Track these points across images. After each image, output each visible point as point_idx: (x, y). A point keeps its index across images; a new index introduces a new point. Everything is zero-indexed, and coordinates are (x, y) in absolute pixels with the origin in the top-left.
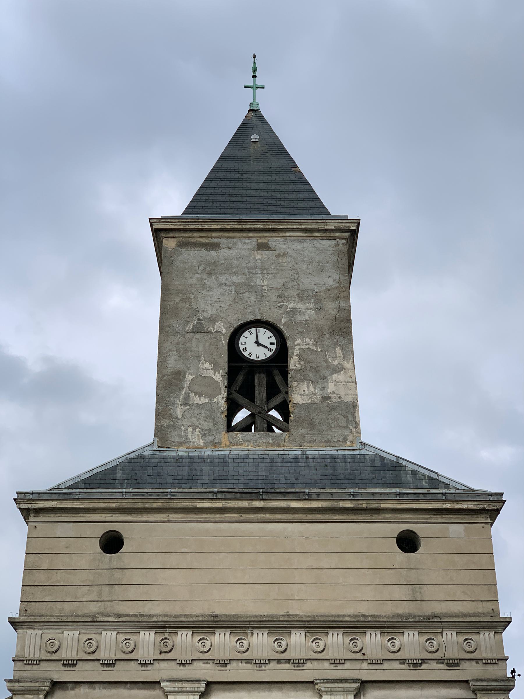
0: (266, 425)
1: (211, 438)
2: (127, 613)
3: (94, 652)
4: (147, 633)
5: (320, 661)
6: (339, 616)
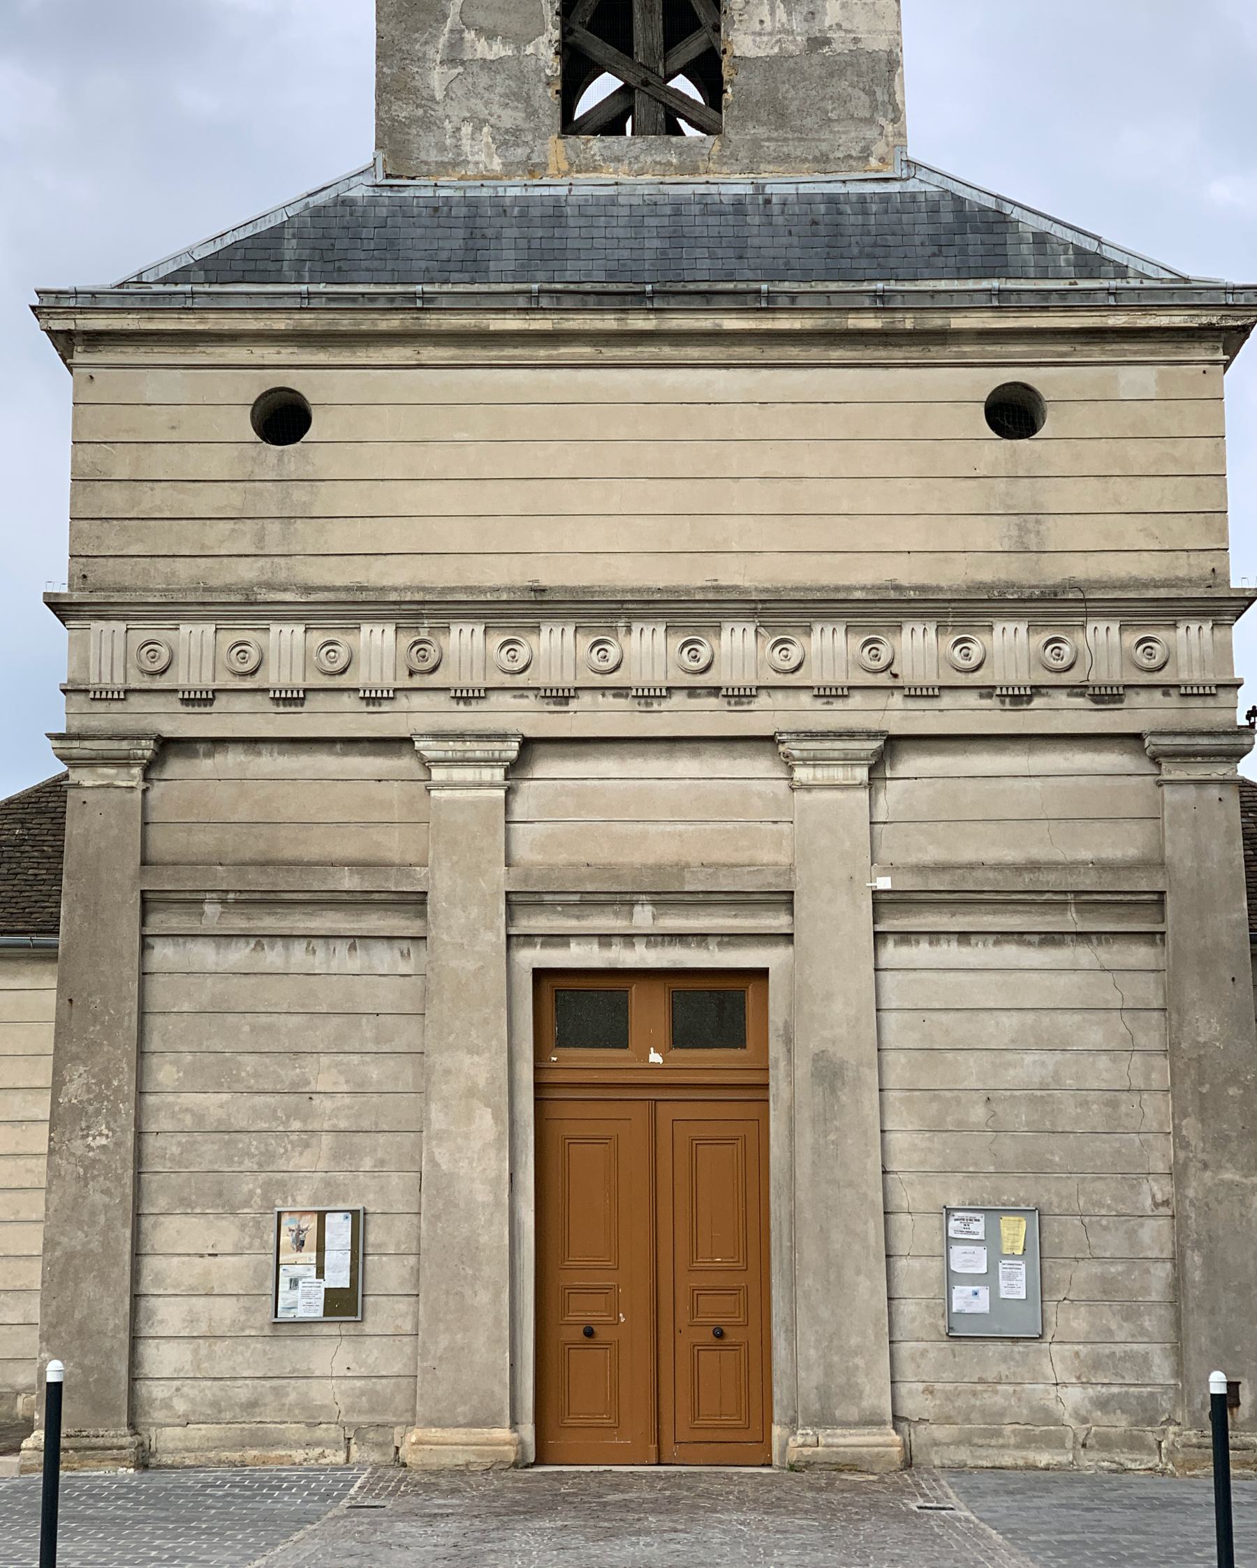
0: (661, 116)
1: (520, 153)
2: (328, 584)
3: (253, 672)
4: (377, 629)
5: (791, 692)
6: (837, 589)
